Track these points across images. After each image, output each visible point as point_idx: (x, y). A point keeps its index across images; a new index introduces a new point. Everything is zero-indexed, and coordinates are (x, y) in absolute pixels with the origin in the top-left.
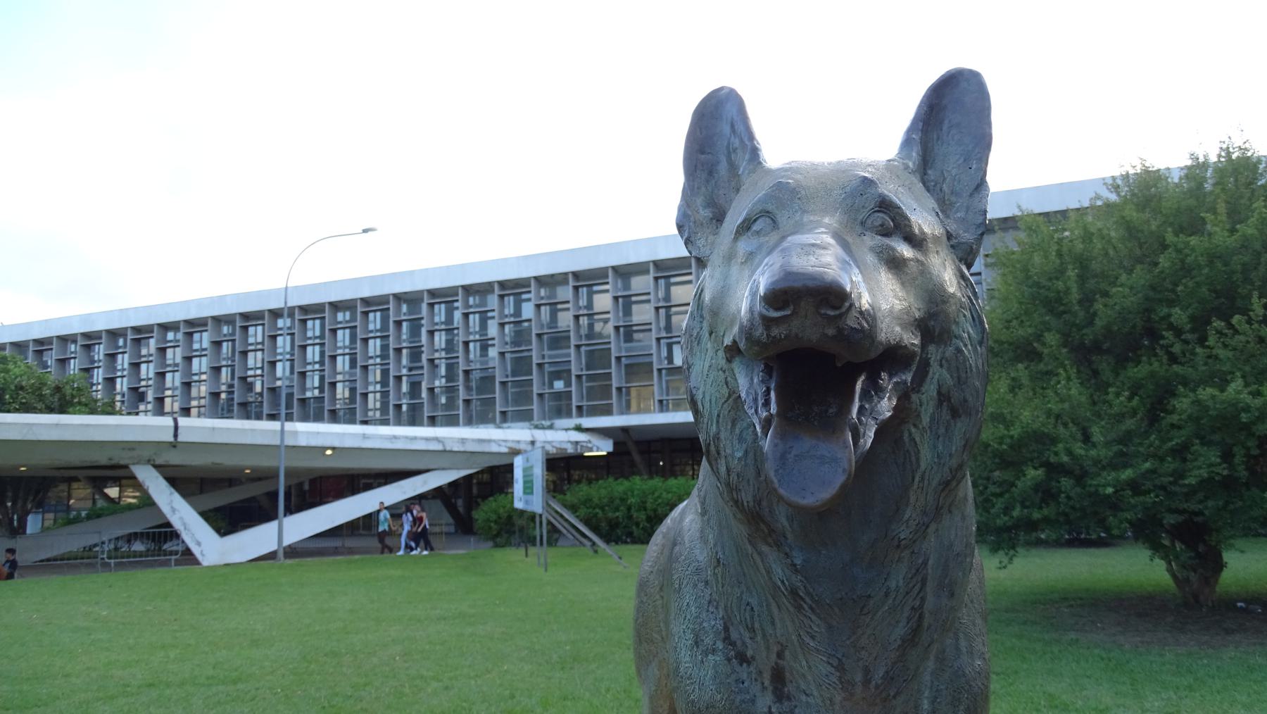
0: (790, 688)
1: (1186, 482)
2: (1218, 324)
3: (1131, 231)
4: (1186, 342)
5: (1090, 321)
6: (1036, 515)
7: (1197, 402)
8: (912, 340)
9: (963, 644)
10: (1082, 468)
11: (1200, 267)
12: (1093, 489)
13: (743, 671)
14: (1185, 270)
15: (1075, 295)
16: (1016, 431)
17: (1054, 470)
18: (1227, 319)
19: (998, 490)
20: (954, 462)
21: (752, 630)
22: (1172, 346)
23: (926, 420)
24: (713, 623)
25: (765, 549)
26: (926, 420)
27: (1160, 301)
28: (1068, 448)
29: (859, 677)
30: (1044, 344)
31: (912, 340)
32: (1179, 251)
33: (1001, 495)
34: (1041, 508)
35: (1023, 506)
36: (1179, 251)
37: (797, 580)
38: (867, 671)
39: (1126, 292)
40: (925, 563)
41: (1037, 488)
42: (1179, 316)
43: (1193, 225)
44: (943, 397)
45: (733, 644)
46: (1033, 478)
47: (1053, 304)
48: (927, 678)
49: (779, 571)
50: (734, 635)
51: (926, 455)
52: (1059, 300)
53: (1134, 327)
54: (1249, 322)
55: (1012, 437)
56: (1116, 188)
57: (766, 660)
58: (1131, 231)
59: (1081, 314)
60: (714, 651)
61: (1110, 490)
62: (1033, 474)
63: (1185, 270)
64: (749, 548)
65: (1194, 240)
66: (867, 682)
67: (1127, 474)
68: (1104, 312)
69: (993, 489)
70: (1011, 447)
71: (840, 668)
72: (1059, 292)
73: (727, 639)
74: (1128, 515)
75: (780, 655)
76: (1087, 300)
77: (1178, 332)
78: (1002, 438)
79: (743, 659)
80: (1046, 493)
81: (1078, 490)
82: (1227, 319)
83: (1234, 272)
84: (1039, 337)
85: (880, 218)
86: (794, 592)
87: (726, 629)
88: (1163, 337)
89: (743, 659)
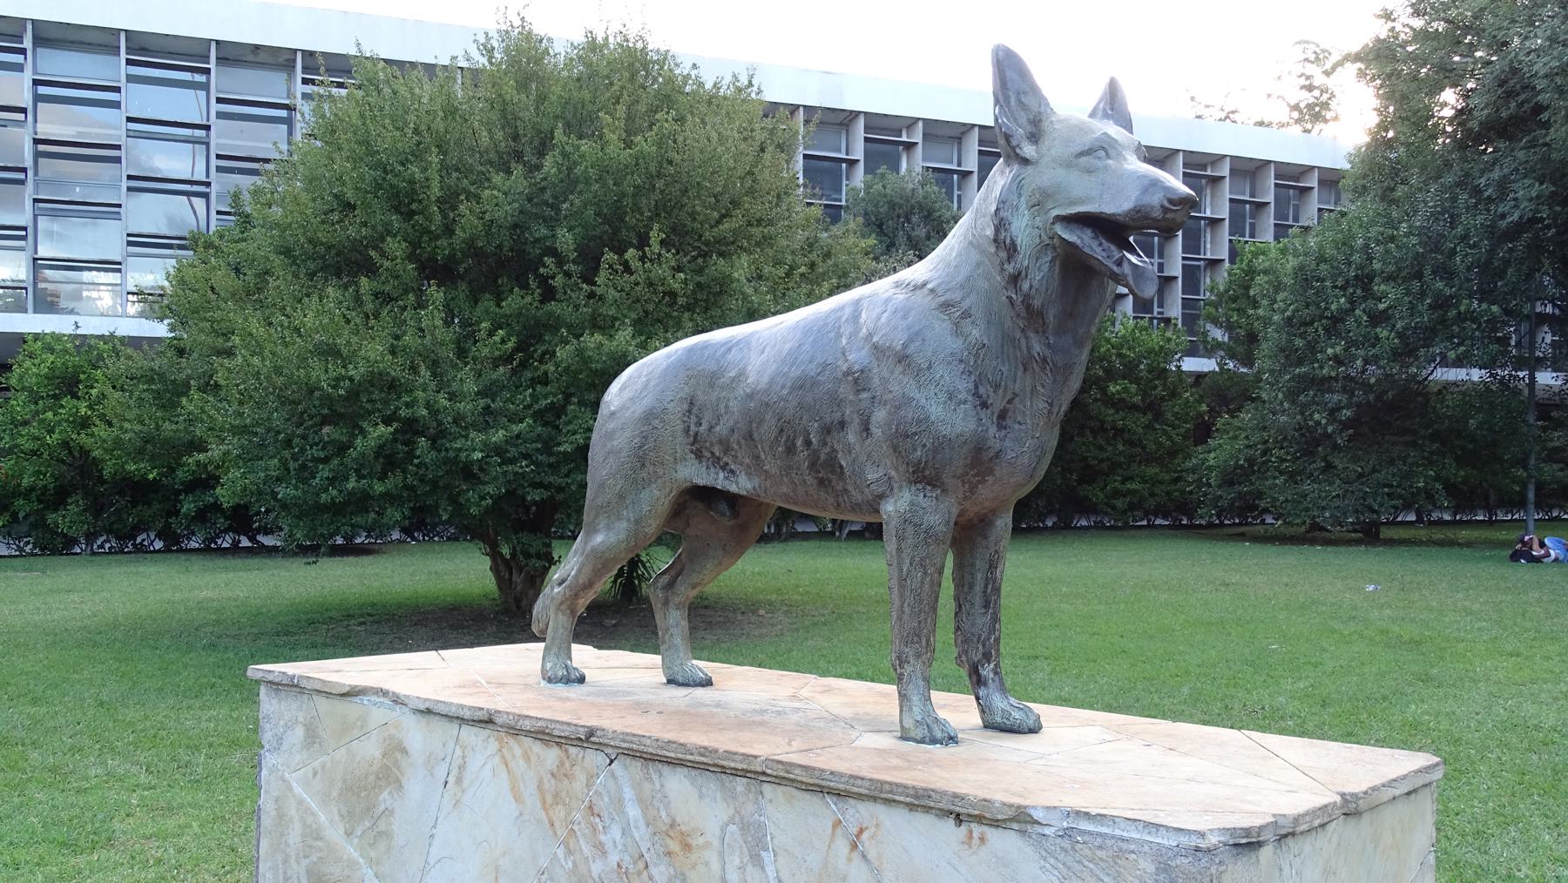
0: (1008, 422)
1: (561, 449)
2: (609, 256)
3: (507, 116)
4: (568, 275)
5: (449, 230)
7: (580, 352)
10: (440, 424)
11: (588, 182)
12: (452, 454)
14: (570, 182)
15: (436, 191)
16: (357, 372)
17: (411, 428)
18: (620, 251)
21: (997, 387)
22: (553, 278)
24: (963, 386)
25: (1032, 335)
27: (537, 217)
28: (423, 397)
30: (383, 254)
32: (565, 155)
33: (326, 460)
35: (360, 477)
36: (565, 155)
37: (1048, 353)
39: (503, 195)
41: (379, 451)
42: (566, 240)
43: (581, 122)
45: (980, 397)
47: (404, 202)
49: (1037, 348)
50: (982, 390)
52: (412, 194)
53: (499, 247)
54: (642, 259)
55: (351, 379)
56: (490, 51)
57: (998, 403)
58: (507, 116)
59: (438, 218)
60: (965, 402)
61: (478, 455)
62: (380, 432)
63: (570, 182)
64: (1018, 335)
65: (585, 146)
67: (498, 436)
68: (468, 219)
71: (1051, 405)
72: (412, 182)
73: (976, 394)
74: (490, 489)
75: (1009, 402)
76: (449, 201)
77: (561, 261)
78: (337, 379)
80: (387, 459)
81: (434, 454)
82: (620, 251)
83: (624, 195)
84: (377, 242)
86: (1044, 360)
87: (976, 387)
88: (544, 266)
89: (984, 405)
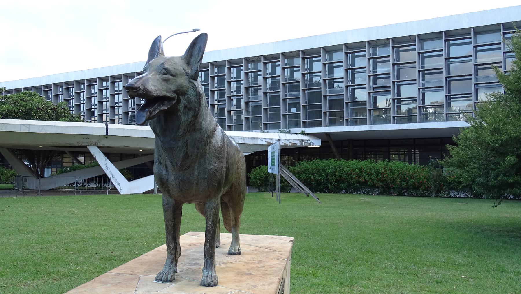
6: (511, 180)
8: (174, 95)
9: (207, 161)
13: (161, 166)
16: (504, 137)
19: (494, 168)
20: (190, 120)
23: (182, 111)
26: (182, 111)
29: (175, 165)
31: (174, 95)
34: (514, 177)
35: (505, 175)
38: (176, 163)
40: (187, 141)
44: (185, 107)
46: (508, 162)
48: (196, 167)
51: (183, 118)
66: (177, 165)
69: (492, 166)
70: (501, 145)
71: (171, 162)
78: (497, 141)
79: (161, 163)
85: (164, 71)
89: (161, 163)
